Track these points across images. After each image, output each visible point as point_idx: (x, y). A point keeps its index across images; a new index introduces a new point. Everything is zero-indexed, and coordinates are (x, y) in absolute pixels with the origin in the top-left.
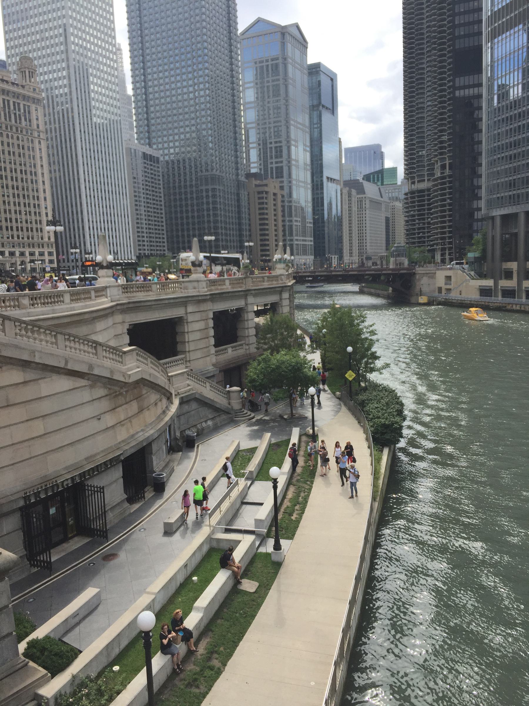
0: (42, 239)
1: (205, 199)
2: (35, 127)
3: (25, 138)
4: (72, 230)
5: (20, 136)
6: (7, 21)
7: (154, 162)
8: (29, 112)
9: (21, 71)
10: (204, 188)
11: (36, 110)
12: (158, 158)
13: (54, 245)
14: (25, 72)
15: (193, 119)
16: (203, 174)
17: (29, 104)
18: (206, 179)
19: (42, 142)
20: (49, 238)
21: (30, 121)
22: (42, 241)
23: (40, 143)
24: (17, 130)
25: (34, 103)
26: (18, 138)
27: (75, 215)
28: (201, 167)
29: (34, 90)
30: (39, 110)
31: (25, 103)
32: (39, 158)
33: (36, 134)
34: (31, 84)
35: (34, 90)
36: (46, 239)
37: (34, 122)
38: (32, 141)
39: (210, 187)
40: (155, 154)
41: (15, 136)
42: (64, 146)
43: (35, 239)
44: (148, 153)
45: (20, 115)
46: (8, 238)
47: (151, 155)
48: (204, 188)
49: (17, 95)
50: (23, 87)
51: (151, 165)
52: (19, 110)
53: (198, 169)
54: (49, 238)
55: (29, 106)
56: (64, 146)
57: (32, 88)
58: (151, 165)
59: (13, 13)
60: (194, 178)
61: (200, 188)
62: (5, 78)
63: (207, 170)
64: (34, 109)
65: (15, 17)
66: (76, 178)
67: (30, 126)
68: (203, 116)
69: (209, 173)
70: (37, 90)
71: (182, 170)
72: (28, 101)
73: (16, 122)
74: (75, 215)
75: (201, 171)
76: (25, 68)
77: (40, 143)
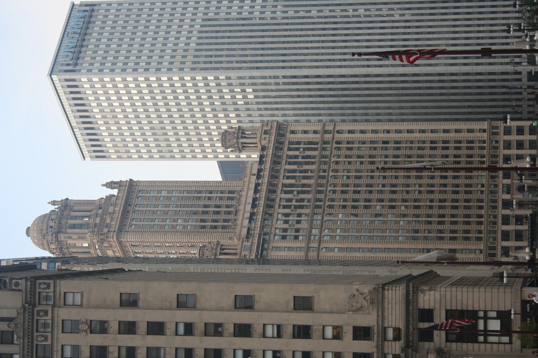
0: (484, 142)
2: (318, 136)
3: (335, 152)
4: (468, 91)
5: (333, 159)
6: (168, 155)
8: (299, 143)
9: (242, 148)
11: (293, 132)
13: (494, 123)
14: (242, 143)
17: (287, 143)
19: (338, 128)
20: (484, 131)
21: (310, 143)
23: (338, 132)
24: (325, 163)
25: (283, 135)
26: (337, 163)
27: (446, 85)
29: (266, 132)
30: (293, 128)
31: (286, 148)
32: (362, 135)
33: (328, 137)
34: (259, 135)
35: (266, 132)
36: (485, 136)
37: (311, 136)
38: (338, 143)
41: (333, 166)
42: (340, 93)
43: (485, 152)
45: (303, 158)
49: (276, 161)
50: (263, 148)
52: (296, 157)
54: (484, 131)
55: (291, 143)
56: (340, 93)
57: (263, 136)
59: (158, 146)
62: (255, 171)
64: (292, 136)
65: (163, 144)
66: (388, 79)
67: (317, 143)
70: (265, 128)
72: (282, 143)
73: (313, 163)
74: (446, 85)
76: (238, 143)
77: (338, 132)
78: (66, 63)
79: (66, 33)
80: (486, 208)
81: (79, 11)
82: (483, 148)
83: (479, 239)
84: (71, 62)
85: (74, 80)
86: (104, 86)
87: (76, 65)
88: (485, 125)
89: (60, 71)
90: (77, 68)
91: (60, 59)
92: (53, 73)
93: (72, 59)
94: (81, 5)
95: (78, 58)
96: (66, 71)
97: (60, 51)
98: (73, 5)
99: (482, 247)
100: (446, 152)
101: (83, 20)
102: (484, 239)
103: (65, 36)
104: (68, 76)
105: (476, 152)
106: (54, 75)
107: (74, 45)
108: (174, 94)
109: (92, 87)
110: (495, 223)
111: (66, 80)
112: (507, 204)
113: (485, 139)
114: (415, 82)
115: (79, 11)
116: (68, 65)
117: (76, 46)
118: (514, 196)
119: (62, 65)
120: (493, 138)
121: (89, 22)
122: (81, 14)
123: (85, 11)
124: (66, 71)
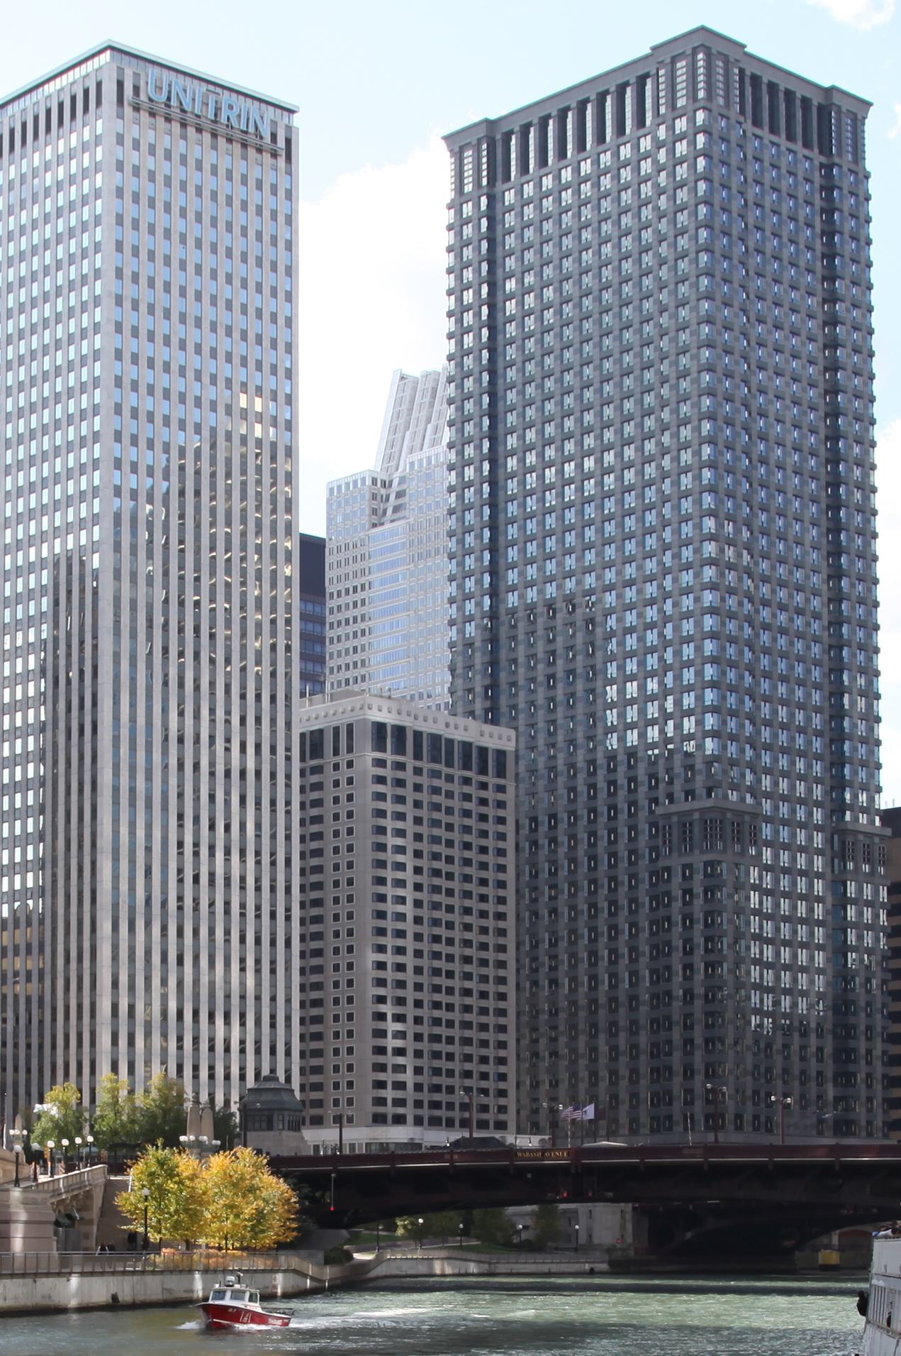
1: (677, 905)
7: (483, 771)
10: (676, 862)
12: (501, 754)
15: (652, 602)
16: (673, 808)
18: (686, 827)
28: (671, 782)
39: (698, 859)
40: (498, 738)
44: (458, 735)
47: (467, 746)
48: (676, 862)
51: (467, 781)
53: (661, 792)
58: (467, 781)
60: (643, 826)
61: (662, 863)
63: (689, 794)
68: (687, 591)
69: (696, 805)
71: (602, 795)
75: (671, 797)
78: (142, 85)
79: (219, 90)
81: (274, 123)
84: (143, 97)
85: (99, 103)
86: (85, 173)
87: (137, 109)
89: (120, 70)
90: (128, 110)
91: (153, 72)
92: (117, 55)
93: (151, 100)
94: (289, 128)
95: (153, 114)
96: (120, 85)
97: (173, 74)
98: (291, 112)
101: (252, 130)
103: (211, 88)
104: (110, 90)
106: (112, 57)
107: (188, 108)
108: (65, 339)
109: (85, 147)
111: (99, 85)
114: (80, 894)
115: (274, 123)
116: (136, 90)
117: (183, 111)
119: (136, 75)
121: (244, 146)
122: (266, 132)
123: (274, 137)
124: (120, 85)
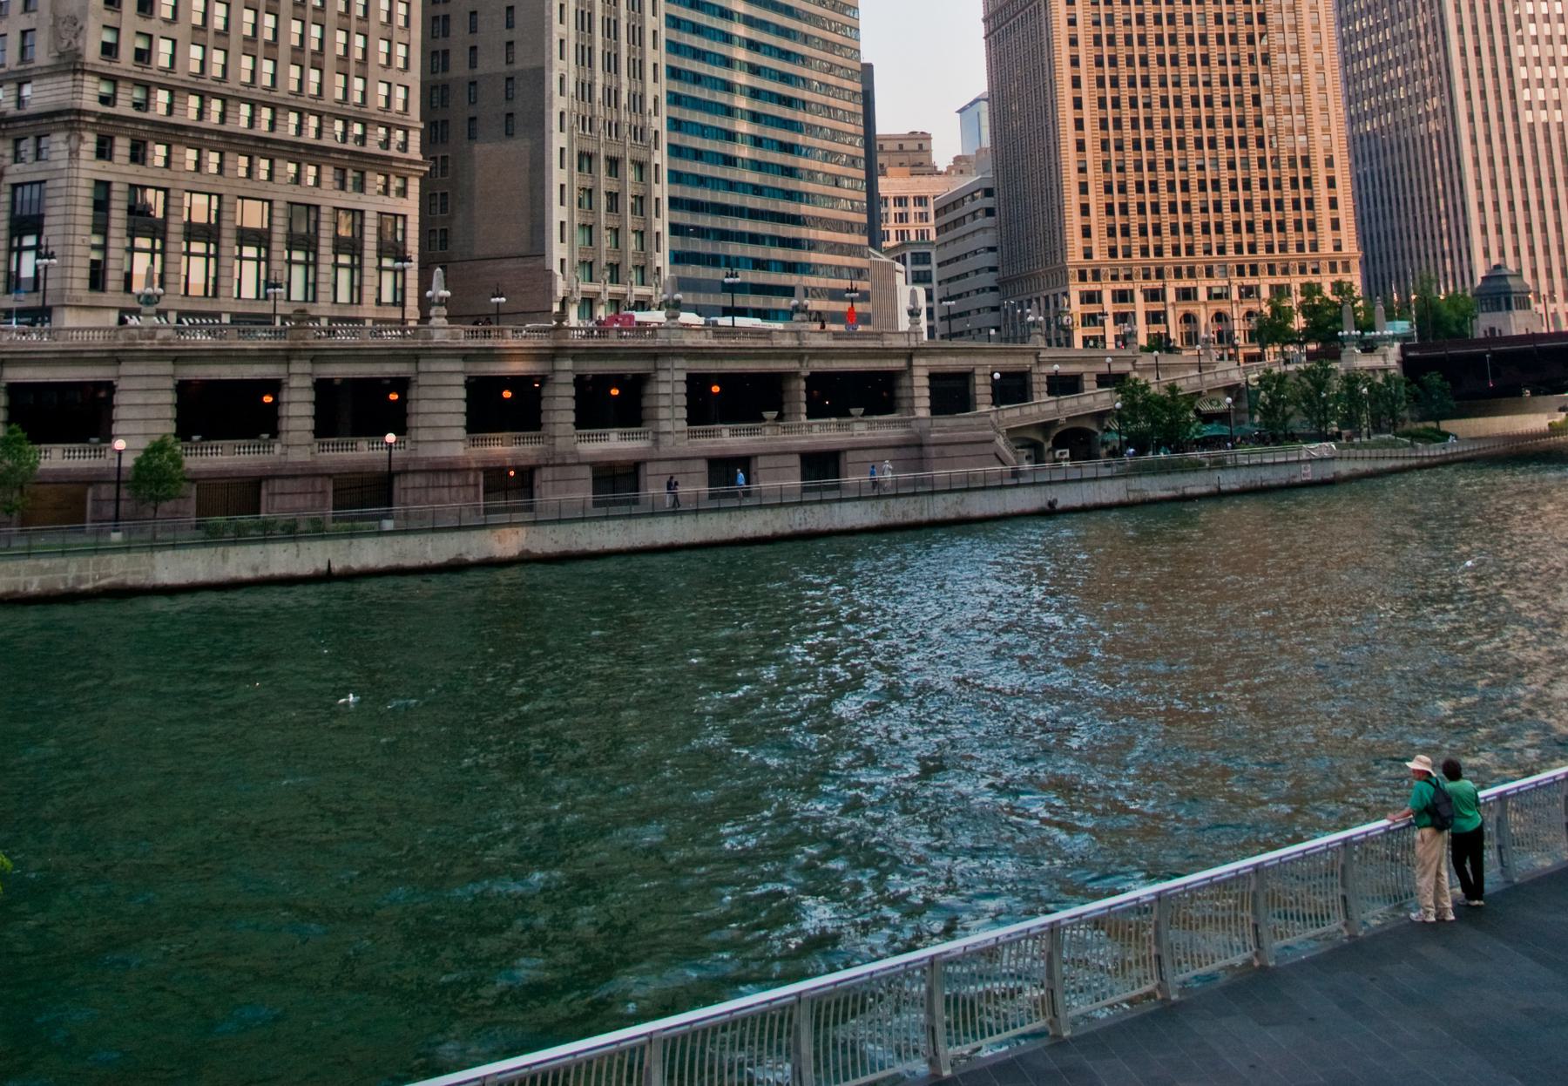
0: (1314, 247)
20: (1338, 248)
22: (1314, 255)
46: (1208, 252)
54: (1338, 248)
80: (1239, 258)
82: (1300, 247)
83: (1113, 252)
88: (1351, 247)
99: (1096, 257)
100: (1286, 185)
102: (1112, 261)
105: (1293, 237)
110: (1115, 278)
112: (1186, 295)
113: (1321, 251)
118: (1202, 308)
120: (1325, 264)
